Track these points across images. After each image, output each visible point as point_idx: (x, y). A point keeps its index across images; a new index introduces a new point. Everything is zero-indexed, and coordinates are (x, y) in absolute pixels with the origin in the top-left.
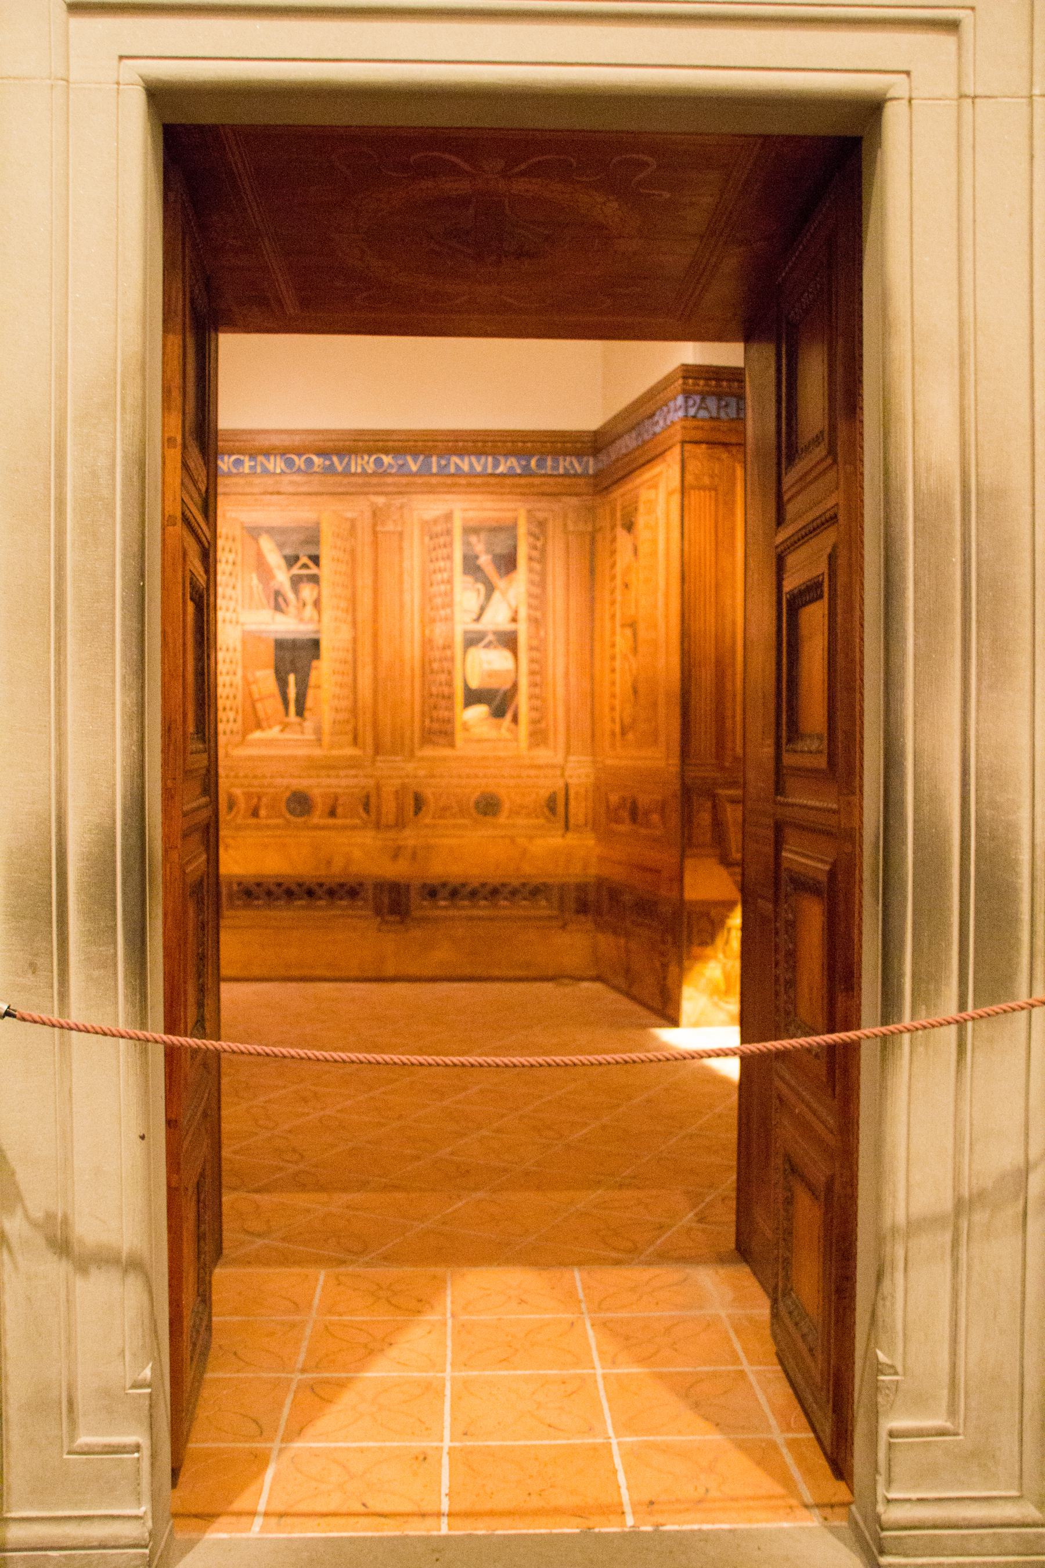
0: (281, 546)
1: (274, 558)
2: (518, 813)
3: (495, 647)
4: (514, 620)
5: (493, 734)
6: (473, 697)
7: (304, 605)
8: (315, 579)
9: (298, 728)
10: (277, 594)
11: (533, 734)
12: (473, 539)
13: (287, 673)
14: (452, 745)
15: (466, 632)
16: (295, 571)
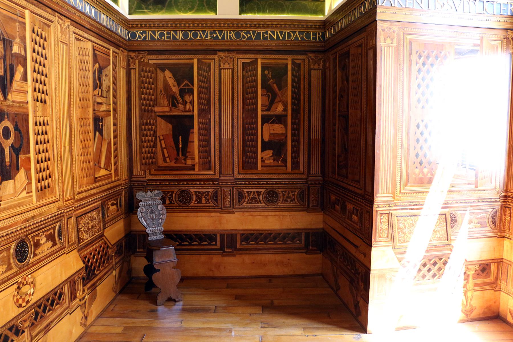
0: (175, 76)
1: (171, 81)
2: (286, 201)
3: (277, 123)
4: (285, 110)
5: (276, 164)
6: (265, 146)
7: (186, 103)
8: (191, 92)
9: (183, 161)
10: (174, 98)
11: (293, 163)
12: (266, 72)
13: (179, 136)
14: (256, 168)
15: (262, 116)
16: (182, 86)
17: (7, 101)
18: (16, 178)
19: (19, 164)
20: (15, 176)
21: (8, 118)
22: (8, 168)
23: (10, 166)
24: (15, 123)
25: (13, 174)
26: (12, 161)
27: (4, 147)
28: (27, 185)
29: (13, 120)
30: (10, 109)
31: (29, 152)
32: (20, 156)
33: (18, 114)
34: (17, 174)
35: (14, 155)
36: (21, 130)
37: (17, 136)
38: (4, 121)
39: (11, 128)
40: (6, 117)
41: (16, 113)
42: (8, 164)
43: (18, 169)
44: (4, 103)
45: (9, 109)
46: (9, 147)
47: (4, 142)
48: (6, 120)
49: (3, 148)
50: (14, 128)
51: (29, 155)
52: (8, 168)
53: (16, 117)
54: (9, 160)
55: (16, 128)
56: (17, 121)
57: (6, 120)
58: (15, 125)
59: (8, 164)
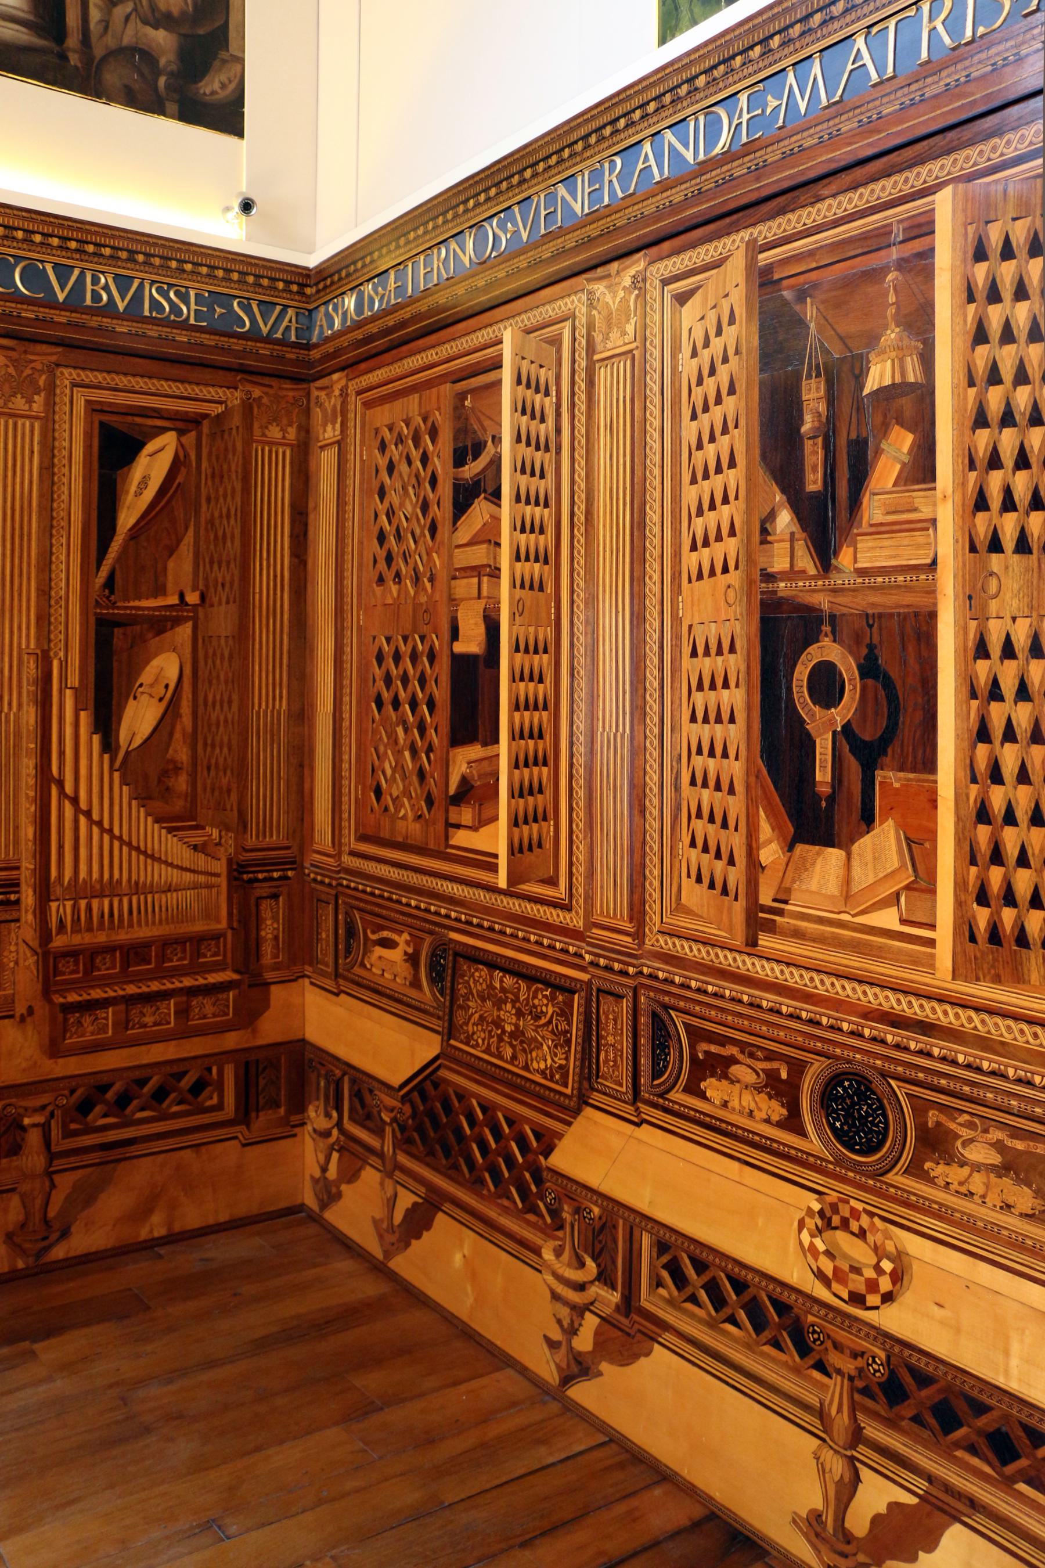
17: (834, 575)
18: (855, 848)
19: (873, 801)
20: (853, 841)
21: (834, 632)
22: (824, 804)
23: (831, 799)
24: (864, 651)
25: (845, 830)
26: (840, 782)
27: (813, 733)
28: (908, 888)
29: (858, 638)
30: (840, 600)
31: (929, 764)
32: (879, 775)
33: (880, 616)
34: (862, 836)
35: (853, 767)
36: (894, 674)
37: (870, 696)
38: (815, 646)
39: (847, 666)
40: (825, 628)
41: (870, 612)
42: (825, 790)
43: (868, 819)
44: (820, 583)
45: (839, 600)
46: (834, 733)
47: (813, 715)
48: (826, 642)
49: (808, 735)
50: (860, 667)
51: (931, 777)
52: (824, 804)
53: (871, 626)
54: (828, 778)
55: (869, 669)
56: (876, 640)
57: (826, 642)
58: (866, 658)
59: (825, 790)
